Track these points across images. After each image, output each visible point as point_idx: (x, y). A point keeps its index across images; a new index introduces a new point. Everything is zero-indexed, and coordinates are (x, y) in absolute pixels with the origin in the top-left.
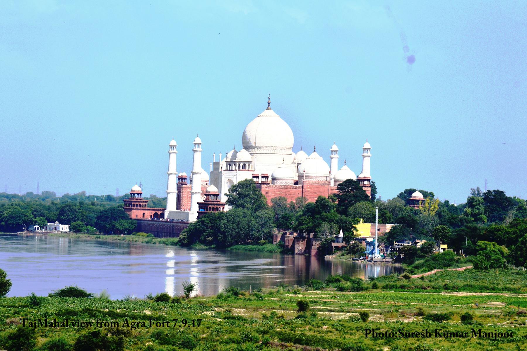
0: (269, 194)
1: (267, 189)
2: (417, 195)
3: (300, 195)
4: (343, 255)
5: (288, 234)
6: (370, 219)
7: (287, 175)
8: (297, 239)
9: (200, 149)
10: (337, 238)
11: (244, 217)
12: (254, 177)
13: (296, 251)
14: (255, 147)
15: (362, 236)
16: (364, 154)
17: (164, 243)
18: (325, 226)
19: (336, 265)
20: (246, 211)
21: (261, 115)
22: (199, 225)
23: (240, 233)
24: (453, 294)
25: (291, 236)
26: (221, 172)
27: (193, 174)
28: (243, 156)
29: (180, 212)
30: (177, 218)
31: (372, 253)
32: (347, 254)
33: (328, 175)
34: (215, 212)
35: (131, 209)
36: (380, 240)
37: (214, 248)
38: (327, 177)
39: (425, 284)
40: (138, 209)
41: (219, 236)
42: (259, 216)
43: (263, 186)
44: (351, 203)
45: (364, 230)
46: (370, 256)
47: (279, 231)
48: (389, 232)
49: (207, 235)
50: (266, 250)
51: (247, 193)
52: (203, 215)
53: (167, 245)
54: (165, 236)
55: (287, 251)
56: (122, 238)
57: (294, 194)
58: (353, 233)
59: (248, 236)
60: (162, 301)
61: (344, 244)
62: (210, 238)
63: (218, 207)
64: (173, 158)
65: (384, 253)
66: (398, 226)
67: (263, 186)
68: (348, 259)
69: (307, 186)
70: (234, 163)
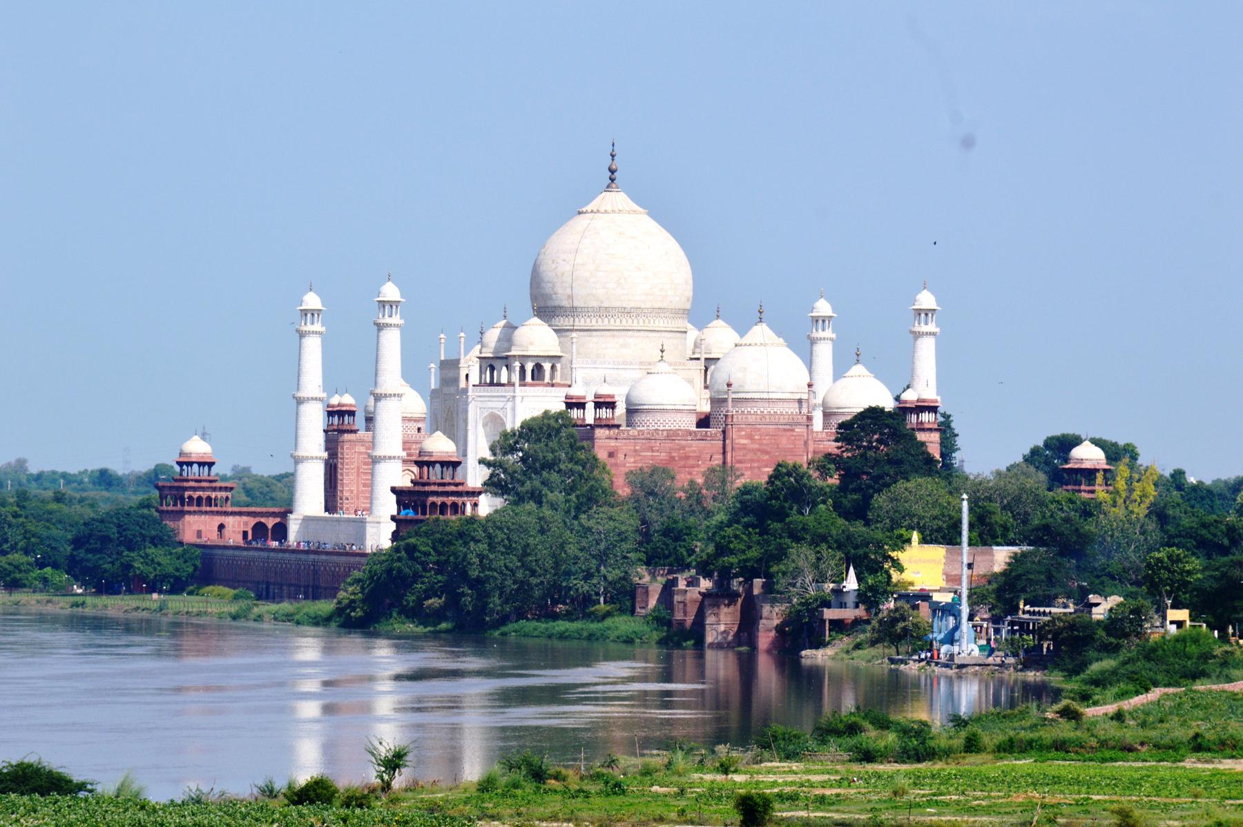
0: (620, 459)
1: (613, 443)
2: (1088, 455)
3: (717, 460)
4: (858, 646)
5: (682, 585)
6: (945, 534)
7: (675, 395)
8: (710, 600)
9: (396, 319)
10: (838, 592)
11: (542, 531)
12: (570, 405)
13: (709, 639)
14: (573, 311)
15: (917, 588)
16: (917, 329)
17: (289, 617)
18: (802, 555)
19: (837, 681)
20: (547, 512)
21: (589, 208)
22: (399, 559)
23: (529, 585)
24: (1221, 767)
25: (693, 589)
26: (465, 391)
27: (378, 398)
28: (536, 338)
29: (338, 520)
30: (330, 540)
31: (951, 639)
32: (873, 643)
33: (805, 396)
34: (450, 516)
35: (182, 513)
36: (976, 598)
37: (447, 631)
38: (800, 401)
39: (1130, 733)
40: (201, 513)
41: (463, 594)
42: (589, 529)
43: (599, 433)
44: (880, 483)
45: (923, 567)
46: (944, 649)
47: (653, 576)
48: (1004, 574)
49: (425, 591)
50: (613, 635)
51: (549, 455)
52: (412, 529)
53: (298, 623)
54: (289, 597)
55: (681, 637)
56: (155, 606)
57: (698, 458)
58: (890, 577)
59: (557, 592)
60: (312, 802)
61: (861, 612)
62: (435, 602)
63: (459, 500)
64: (313, 350)
65: (989, 640)
66: (1030, 553)
67: (599, 433)
68: (875, 661)
69: (740, 430)
70: (507, 361)
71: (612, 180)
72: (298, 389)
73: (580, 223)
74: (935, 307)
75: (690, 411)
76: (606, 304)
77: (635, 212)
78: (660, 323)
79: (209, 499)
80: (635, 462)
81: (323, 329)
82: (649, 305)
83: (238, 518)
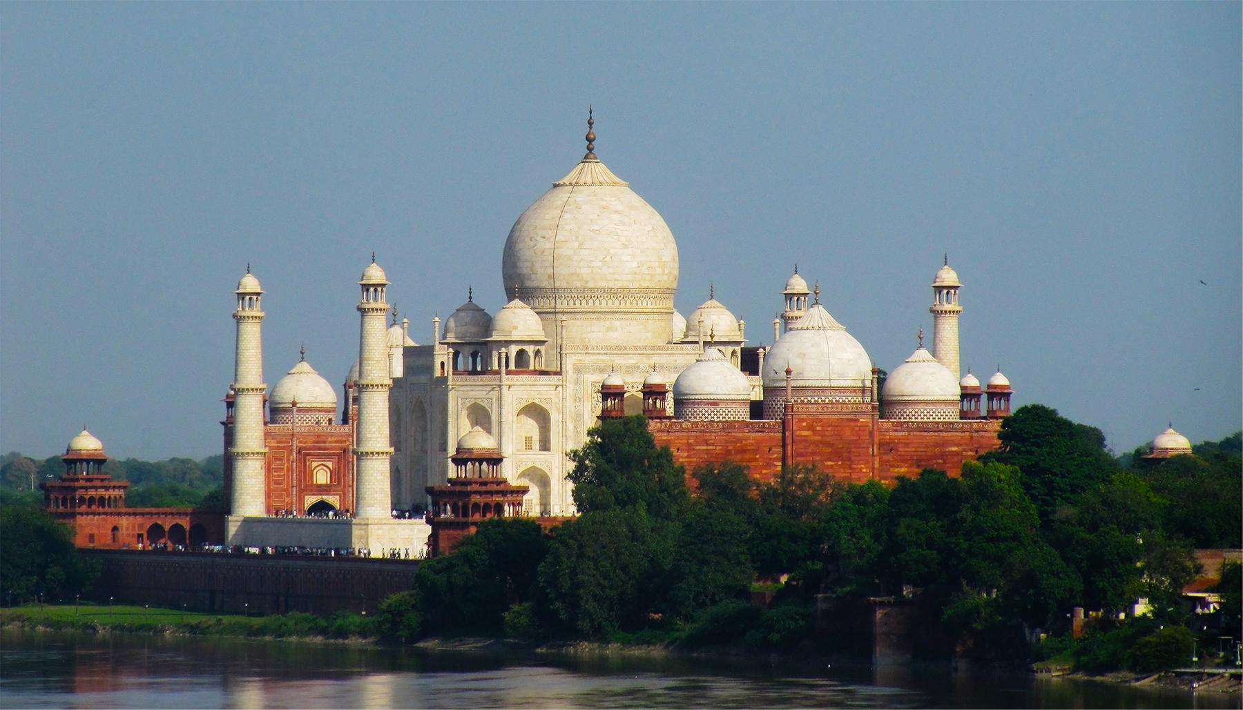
21: (566, 180)
26: (443, 380)
35: (73, 515)
40: (94, 514)
57: (756, 451)
71: (590, 150)
72: (236, 380)
73: (562, 195)
74: (384, 282)
75: (743, 402)
76: (591, 285)
77: (615, 184)
78: (649, 305)
79: (102, 501)
80: (688, 457)
81: (262, 314)
82: (636, 285)
83: (132, 518)
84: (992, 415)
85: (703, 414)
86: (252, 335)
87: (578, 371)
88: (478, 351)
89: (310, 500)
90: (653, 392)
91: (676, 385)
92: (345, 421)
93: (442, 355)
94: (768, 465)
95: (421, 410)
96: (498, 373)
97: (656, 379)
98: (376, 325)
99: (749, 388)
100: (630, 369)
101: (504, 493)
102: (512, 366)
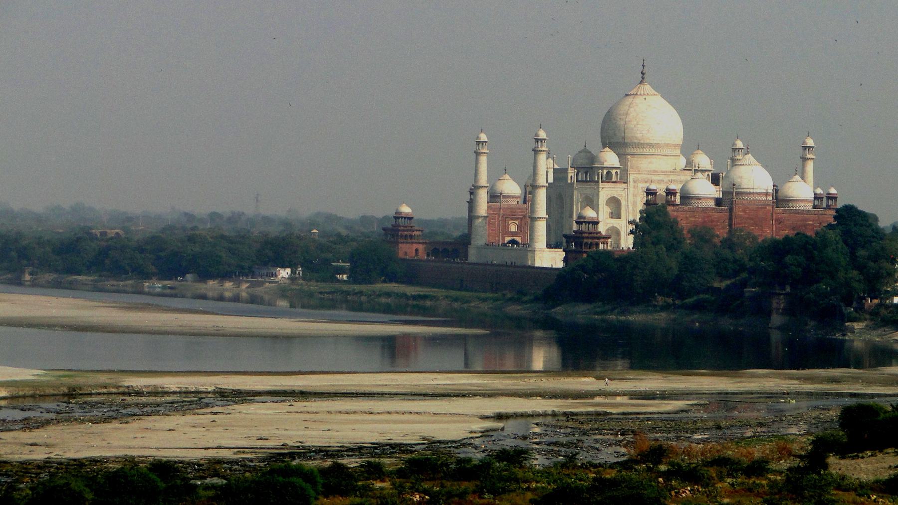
14: (625, 145)
35: (398, 243)
57: (718, 221)
71: (643, 78)
73: (630, 99)
84: (828, 207)
85: (695, 204)
86: (483, 159)
87: (635, 182)
88: (589, 171)
89: (508, 239)
90: (670, 192)
91: (682, 189)
92: (525, 202)
93: (571, 173)
94: (723, 228)
95: (560, 198)
96: (598, 182)
97: (672, 187)
98: (542, 157)
99: (714, 192)
100: (659, 182)
101: (599, 238)
102: (604, 179)
